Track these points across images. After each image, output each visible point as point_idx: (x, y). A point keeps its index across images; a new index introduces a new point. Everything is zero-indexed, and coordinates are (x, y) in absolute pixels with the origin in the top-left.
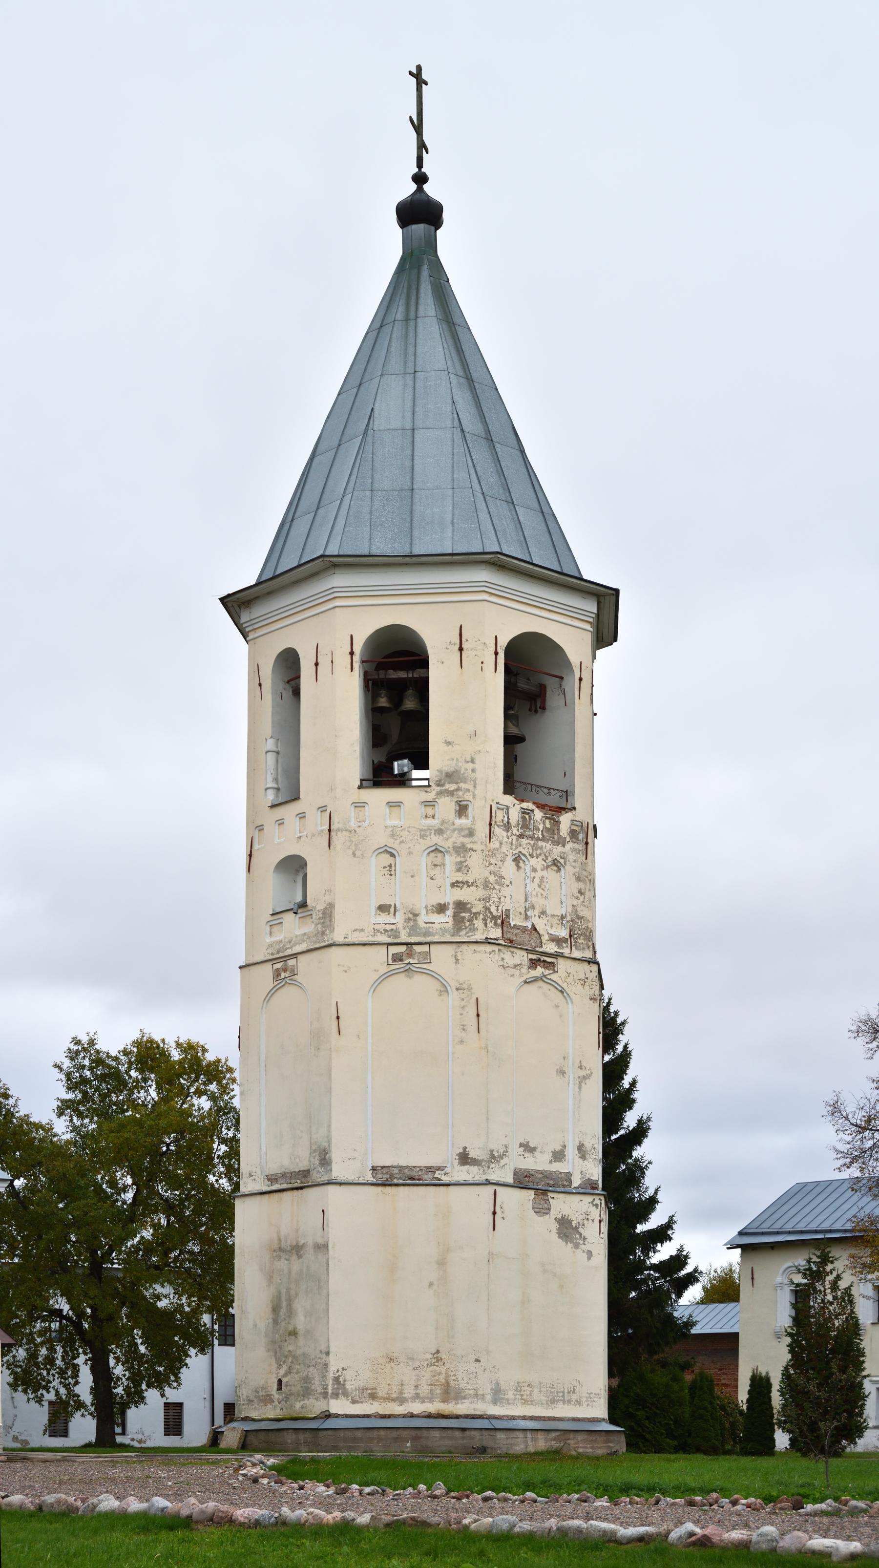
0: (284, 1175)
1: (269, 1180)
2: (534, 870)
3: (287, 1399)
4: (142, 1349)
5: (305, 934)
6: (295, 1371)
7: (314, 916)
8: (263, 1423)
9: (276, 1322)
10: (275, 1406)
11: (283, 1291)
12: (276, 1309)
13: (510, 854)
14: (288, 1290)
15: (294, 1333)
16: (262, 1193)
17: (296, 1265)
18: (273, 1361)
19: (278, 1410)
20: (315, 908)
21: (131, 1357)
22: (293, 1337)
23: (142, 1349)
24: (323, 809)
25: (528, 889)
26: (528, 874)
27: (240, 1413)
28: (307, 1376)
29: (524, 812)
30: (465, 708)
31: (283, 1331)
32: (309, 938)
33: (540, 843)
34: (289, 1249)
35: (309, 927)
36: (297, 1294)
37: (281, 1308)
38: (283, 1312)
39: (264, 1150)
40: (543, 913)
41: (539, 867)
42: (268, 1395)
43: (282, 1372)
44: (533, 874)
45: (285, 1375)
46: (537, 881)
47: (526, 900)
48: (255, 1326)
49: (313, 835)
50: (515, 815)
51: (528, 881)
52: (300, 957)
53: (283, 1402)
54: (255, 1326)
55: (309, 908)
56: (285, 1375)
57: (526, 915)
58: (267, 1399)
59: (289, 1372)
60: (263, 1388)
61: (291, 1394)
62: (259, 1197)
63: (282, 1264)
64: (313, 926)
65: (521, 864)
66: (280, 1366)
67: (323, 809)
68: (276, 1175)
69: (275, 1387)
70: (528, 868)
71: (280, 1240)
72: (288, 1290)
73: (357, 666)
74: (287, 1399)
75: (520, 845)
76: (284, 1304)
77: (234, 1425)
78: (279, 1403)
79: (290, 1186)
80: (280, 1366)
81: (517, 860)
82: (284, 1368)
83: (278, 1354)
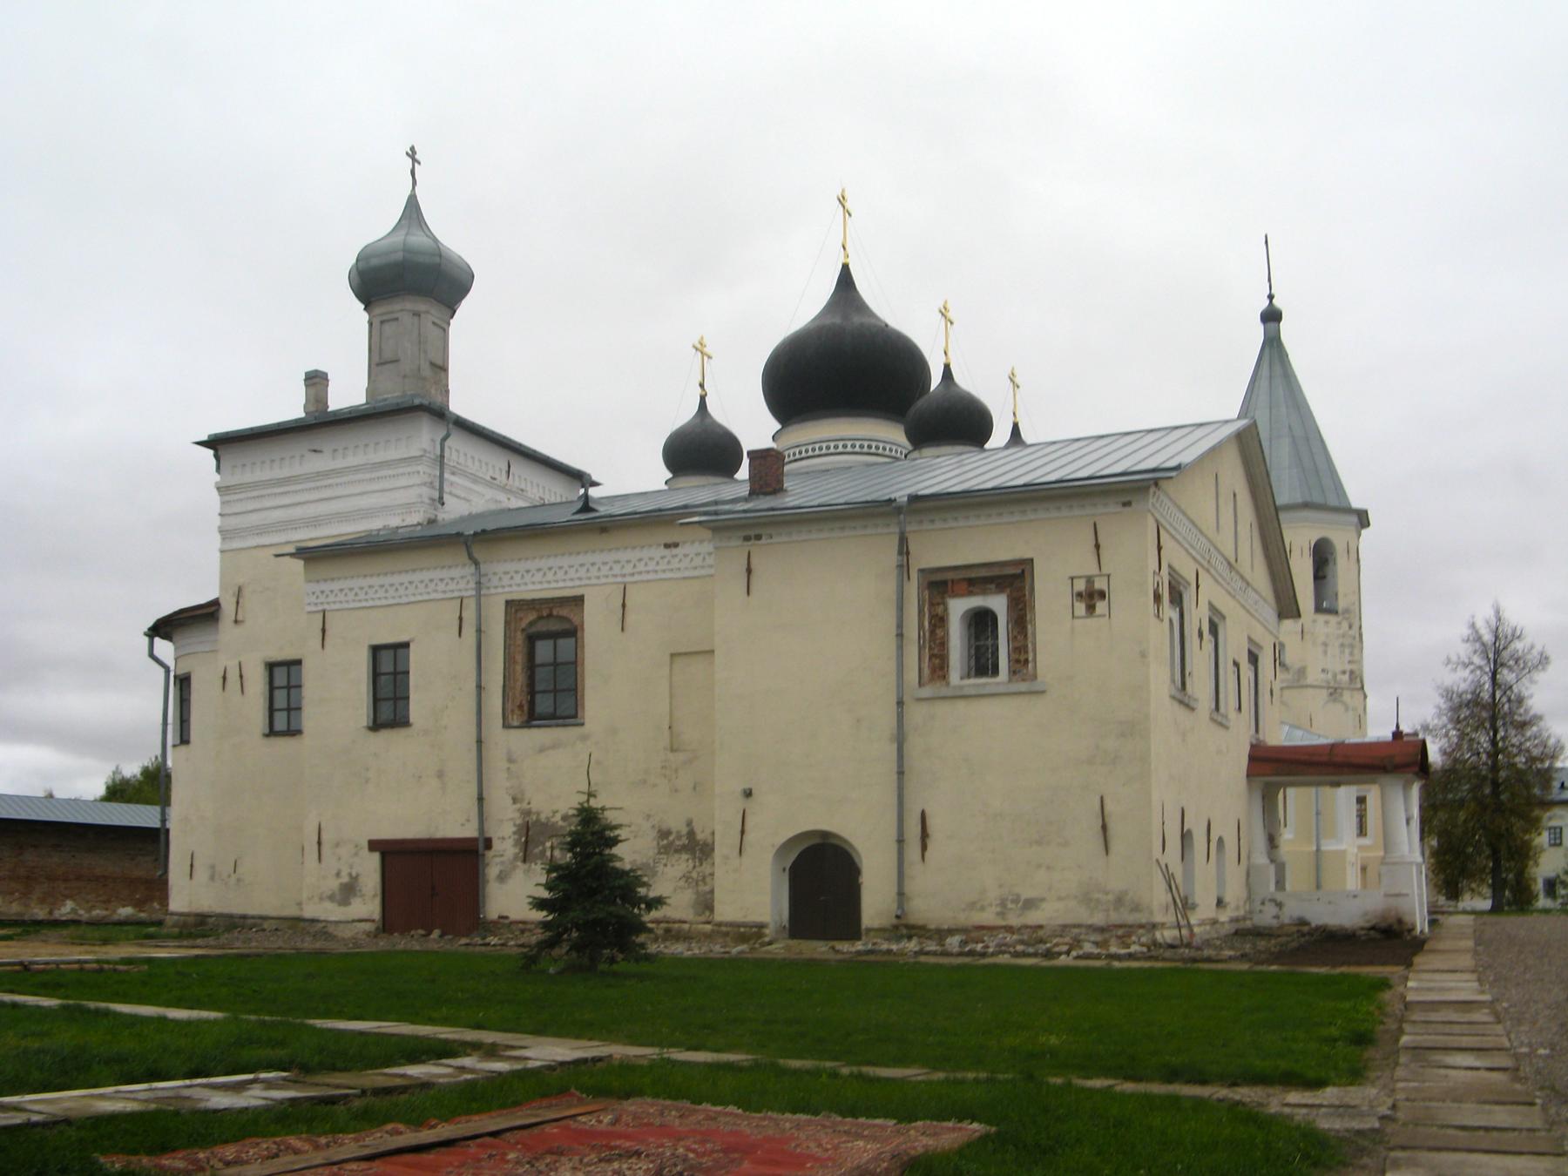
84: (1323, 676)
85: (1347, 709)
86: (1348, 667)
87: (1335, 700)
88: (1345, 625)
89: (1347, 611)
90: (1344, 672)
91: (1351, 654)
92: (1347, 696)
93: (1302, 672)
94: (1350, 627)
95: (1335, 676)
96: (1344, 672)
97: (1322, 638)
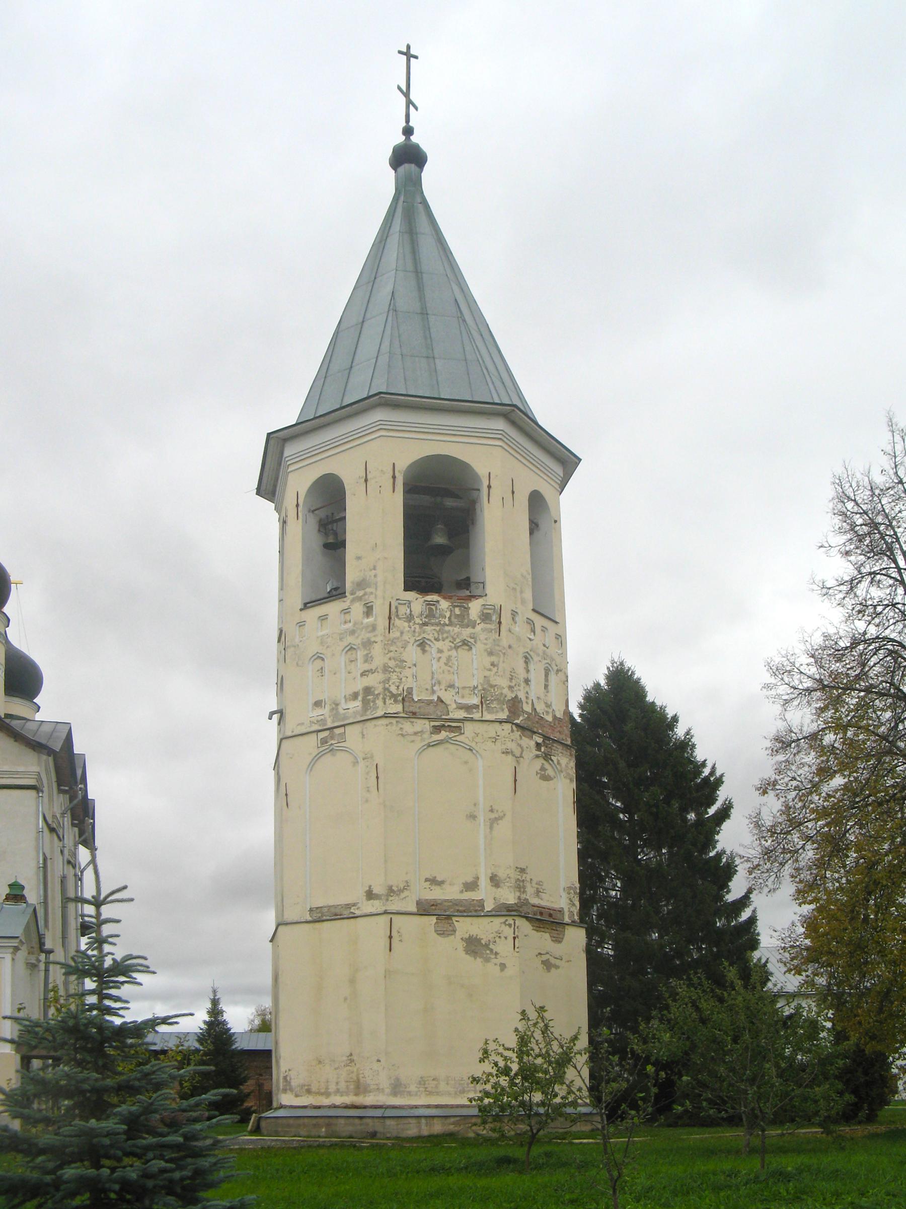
2: (440, 651)
25: (435, 668)
29: (429, 604)
40: (452, 686)
41: (445, 649)
44: (439, 655)
46: (444, 660)
47: (433, 678)
65: (427, 648)
70: (434, 651)
81: (422, 645)
84: (319, 711)
85: (356, 763)
86: (359, 685)
88: (358, 609)
89: (361, 584)
90: (355, 696)
91: (368, 659)
94: (369, 610)
96: (355, 696)
97: (314, 647)
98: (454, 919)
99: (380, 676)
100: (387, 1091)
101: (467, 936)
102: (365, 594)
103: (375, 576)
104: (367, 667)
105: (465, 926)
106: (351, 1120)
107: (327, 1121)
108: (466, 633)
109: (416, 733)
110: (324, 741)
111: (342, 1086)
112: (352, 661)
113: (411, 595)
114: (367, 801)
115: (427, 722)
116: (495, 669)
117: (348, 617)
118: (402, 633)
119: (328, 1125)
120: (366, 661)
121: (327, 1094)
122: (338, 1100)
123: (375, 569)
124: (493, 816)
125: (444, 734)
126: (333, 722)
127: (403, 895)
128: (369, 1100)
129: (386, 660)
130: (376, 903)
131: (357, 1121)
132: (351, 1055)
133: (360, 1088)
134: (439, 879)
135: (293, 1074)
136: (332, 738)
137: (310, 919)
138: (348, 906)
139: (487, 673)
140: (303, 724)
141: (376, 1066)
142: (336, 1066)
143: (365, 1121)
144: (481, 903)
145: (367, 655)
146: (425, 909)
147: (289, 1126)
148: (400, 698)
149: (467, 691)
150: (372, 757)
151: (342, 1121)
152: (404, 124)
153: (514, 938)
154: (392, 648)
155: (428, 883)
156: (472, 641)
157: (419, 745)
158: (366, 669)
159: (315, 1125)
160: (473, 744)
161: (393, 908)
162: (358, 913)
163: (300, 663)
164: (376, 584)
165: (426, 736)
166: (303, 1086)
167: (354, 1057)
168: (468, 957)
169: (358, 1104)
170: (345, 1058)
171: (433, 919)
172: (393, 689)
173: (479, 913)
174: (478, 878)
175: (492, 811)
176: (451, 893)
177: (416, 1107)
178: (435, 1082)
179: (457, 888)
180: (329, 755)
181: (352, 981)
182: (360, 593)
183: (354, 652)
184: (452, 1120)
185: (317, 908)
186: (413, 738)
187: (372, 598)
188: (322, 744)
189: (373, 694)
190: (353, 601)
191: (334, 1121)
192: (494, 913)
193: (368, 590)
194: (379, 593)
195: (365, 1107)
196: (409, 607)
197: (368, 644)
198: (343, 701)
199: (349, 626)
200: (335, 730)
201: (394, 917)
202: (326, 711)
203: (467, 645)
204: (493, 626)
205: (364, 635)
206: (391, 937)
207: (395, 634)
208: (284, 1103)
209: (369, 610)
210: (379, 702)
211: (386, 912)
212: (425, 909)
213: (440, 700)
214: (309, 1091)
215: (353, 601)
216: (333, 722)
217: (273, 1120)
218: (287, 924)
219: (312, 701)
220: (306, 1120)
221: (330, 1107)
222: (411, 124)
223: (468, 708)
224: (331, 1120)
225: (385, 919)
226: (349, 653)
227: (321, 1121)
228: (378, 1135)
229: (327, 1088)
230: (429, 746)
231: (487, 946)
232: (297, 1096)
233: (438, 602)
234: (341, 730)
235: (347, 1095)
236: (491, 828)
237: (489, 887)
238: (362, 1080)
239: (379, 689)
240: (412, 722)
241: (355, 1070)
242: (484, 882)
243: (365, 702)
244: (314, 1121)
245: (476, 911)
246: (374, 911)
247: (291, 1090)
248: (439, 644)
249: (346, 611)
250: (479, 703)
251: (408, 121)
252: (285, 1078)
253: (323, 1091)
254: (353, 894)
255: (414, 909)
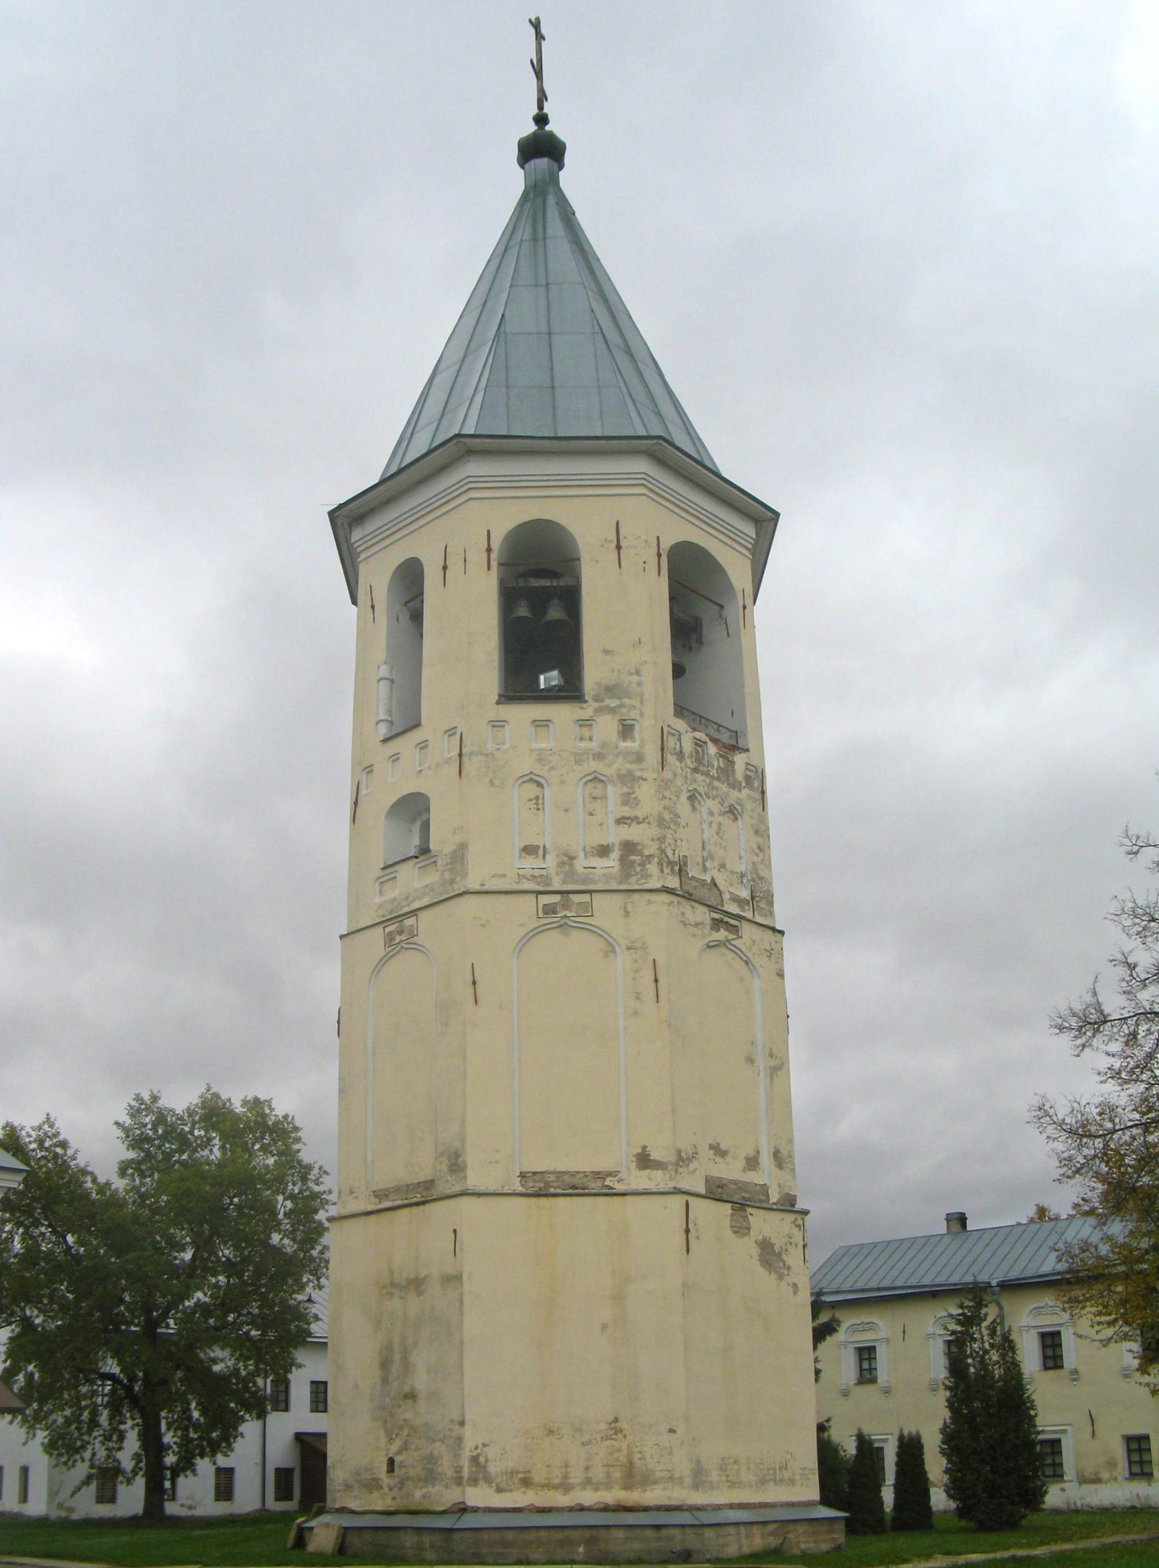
0: (398, 1189)
1: (376, 1196)
2: (711, 814)
3: (401, 1485)
4: (196, 1414)
5: (427, 886)
6: (413, 1447)
7: (439, 863)
8: (367, 1517)
9: (385, 1381)
10: (385, 1495)
11: (396, 1340)
12: (385, 1365)
13: (684, 788)
14: (403, 1339)
15: (411, 1396)
16: (368, 1214)
17: (415, 1305)
18: (382, 1434)
19: (389, 1501)
20: (440, 852)
21: (183, 1424)
22: (410, 1402)
23: (196, 1414)
24: (450, 732)
25: (705, 835)
26: (705, 817)
27: (334, 1500)
28: (431, 1454)
29: (698, 743)
30: (624, 618)
31: (396, 1394)
32: (432, 890)
33: (716, 783)
34: (404, 1284)
35: (433, 877)
36: (415, 1344)
37: (391, 1363)
38: (396, 1368)
39: (370, 1158)
40: (723, 866)
41: (716, 812)
42: (373, 1479)
43: (394, 1448)
44: (711, 819)
45: (399, 1452)
46: (715, 827)
47: (703, 848)
48: (356, 1386)
49: (438, 765)
50: (688, 746)
51: (705, 826)
52: (421, 914)
53: (396, 1490)
54: (356, 1386)
55: (433, 853)
56: (399, 1452)
57: (704, 866)
58: (373, 1485)
59: (405, 1447)
60: (366, 1469)
61: (408, 1478)
62: (363, 1219)
63: (395, 1304)
64: (438, 874)
65: (696, 805)
66: (391, 1440)
67: (450, 732)
68: (387, 1189)
69: (385, 1468)
70: (704, 811)
71: (392, 1273)
72: (403, 1339)
73: (494, 564)
74: (401, 1485)
75: (695, 781)
76: (397, 1357)
77: (324, 1518)
78: (390, 1490)
79: (406, 1202)
80: (391, 1440)
81: (692, 798)
82: (397, 1444)
83: (388, 1424)
84: (530, 863)
85: (610, 950)
86: (615, 836)
87: (563, 927)
88: (606, 727)
89: (611, 690)
90: (603, 851)
91: (628, 799)
92: (606, 910)
93: (459, 855)
94: (627, 730)
95: (568, 859)
96: (603, 851)
97: (527, 765)
98: (749, 1210)
99: (655, 831)
100: (688, 1481)
101: (760, 1238)
102: (622, 706)
103: (639, 684)
104: (626, 811)
105: (764, 1224)
106: (638, 1531)
107: (588, 1533)
108: (734, 795)
109: (697, 925)
110: (549, 910)
111: (598, 1473)
112: (595, 798)
113: (680, 725)
114: (636, 1013)
115: (705, 909)
116: (761, 855)
117: (586, 732)
118: (675, 775)
119: (590, 1541)
120: (625, 803)
121: (565, 1487)
122: (588, 1497)
123: (638, 673)
124: (773, 1063)
125: (722, 934)
126: (564, 882)
127: (692, 1166)
128: (653, 1496)
129: (661, 809)
130: (658, 1174)
131: (649, 1533)
132: (616, 1420)
133: (632, 1476)
134: (723, 1147)
135: (492, 1453)
136: (566, 906)
137: (520, 1189)
138: (599, 1176)
139: (755, 859)
140: (503, 876)
141: (665, 1439)
142: (586, 1437)
143: (664, 1532)
144: (764, 1188)
145: (629, 794)
146: (716, 1192)
147: (505, 1543)
148: (677, 868)
149: (735, 878)
150: (644, 948)
151: (621, 1534)
152: (535, 111)
153: (804, 1246)
154: (667, 794)
155: (712, 1152)
156: (739, 808)
157: (701, 943)
158: (628, 815)
159: (562, 1543)
160: (750, 955)
161: (684, 1185)
162: (619, 1187)
163: (497, 782)
164: (642, 696)
165: (707, 930)
166: (513, 1473)
167: (623, 1424)
168: (762, 1269)
169: (630, 1504)
170: (603, 1426)
171: (729, 1206)
172: (669, 852)
173: (766, 1205)
174: (758, 1152)
175: (771, 1055)
176: (731, 1170)
177: (719, 1507)
178: (736, 1467)
179: (740, 1163)
180: (558, 931)
181: (619, 1298)
182: (613, 703)
183: (600, 786)
184: (771, 1527)
185: (534, 1173)
186: (695, 930)
187: (634, 714)
188: (545, 913)
189: (641, 853)
190: (598, 711)
191: (603, 1533)
192: (779, 1207)
193: (626, 701)
194: (648, 709)
195: (646, 1509)
196: (680, 740)
197: (628, 779)
198: (582, 855)
199: (594, 745)
200: (572, 896)
201: (691, 1199)
202: (551, 862)
203: (733, 814)
204: (757, 795)
205: (621, 765)
206: (687, 1231)
207: (668, 775)
208: (471, 1502)
209: (627, 730)
210: (653, 868)
211: (677, 1191)
212: (716, 1192)
213: (714, 883)
214: (526, 1482)
215: (598, 711)
216: (564, 882)
217: (469, 1534)
218: (479, 1195)
219: (519, 844)
220: (543, 1534)
221: (571, 1509)
222: (545, 111)
223: (741, 902)
224: (594, 1532)
225: (680, 1200)
226: (590, 785)
227: (574, 1534)
228: (695, 1556)
229: (566, 1477)
230: (709, 947)
231: (779, 1254)
232: (499, 1490)
233: (705, 743)
234: (585, 898)
235: (608, 1486)
236: (772, 1079)
237: (773, 1167)
238: (638, 1463)
239: (652, 849)
240: (693, 907)
241: (624, 1445)
242: (766, 1160)
243: (626, 865)
244: (561, 1535)
245: (761, 1201)
246: (652, 1186)
247: (488, 1480)
248: (710, 803)
249: (583, 723)
250: (749, 898)
251: (541, 107)
252: (475, 1460)
253: (556, 1481)
254: (610, 1155)
255: (703, 1191)
